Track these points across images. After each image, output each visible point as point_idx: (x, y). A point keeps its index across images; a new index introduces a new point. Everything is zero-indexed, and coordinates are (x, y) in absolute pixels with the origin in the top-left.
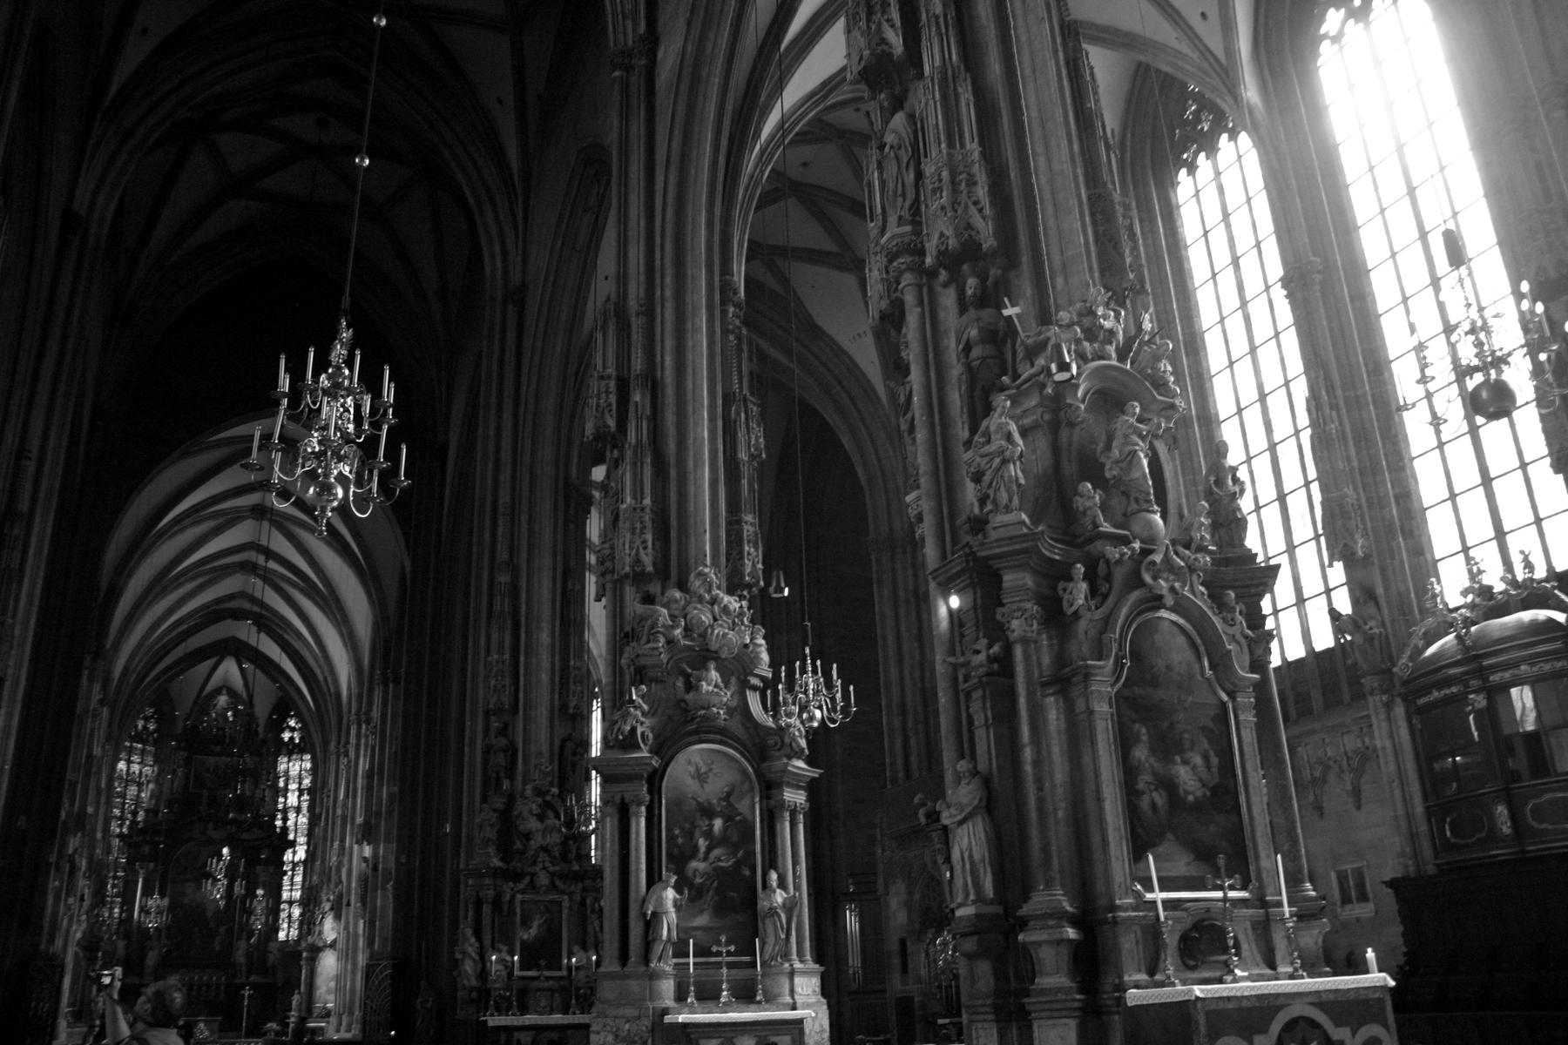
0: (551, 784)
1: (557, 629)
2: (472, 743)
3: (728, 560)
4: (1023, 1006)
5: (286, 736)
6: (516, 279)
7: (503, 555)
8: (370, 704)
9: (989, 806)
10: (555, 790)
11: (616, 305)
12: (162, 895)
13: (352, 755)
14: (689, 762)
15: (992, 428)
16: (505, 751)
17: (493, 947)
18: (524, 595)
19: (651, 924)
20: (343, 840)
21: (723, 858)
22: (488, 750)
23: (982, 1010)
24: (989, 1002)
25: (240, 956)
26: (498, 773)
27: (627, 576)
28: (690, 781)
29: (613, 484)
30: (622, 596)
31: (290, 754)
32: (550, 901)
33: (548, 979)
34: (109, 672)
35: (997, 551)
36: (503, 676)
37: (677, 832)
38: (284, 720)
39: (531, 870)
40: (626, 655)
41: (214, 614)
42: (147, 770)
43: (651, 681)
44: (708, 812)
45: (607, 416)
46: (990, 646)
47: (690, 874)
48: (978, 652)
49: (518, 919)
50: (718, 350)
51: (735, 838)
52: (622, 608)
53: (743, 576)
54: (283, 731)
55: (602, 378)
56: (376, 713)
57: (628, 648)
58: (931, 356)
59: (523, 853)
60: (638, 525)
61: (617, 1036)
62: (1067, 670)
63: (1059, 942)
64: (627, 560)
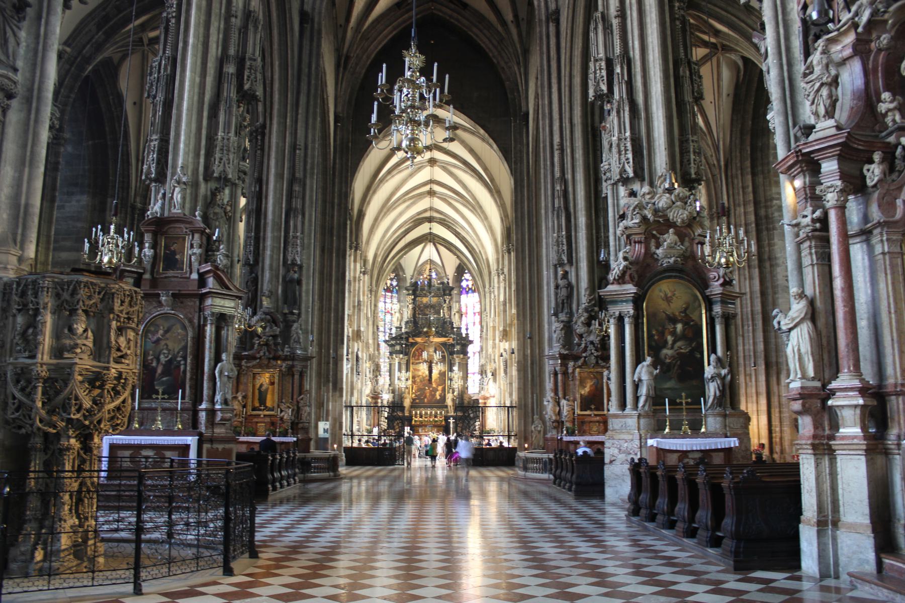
0: (594, 305)
1: (593, 214)
2: (548, 284)
3: (681, 165)
4: (830, 446)
5: (464, 284)
6: (552, 6)
7: (557, 174)
8: (503, 264)
9: (812, 315)
10: (596, 309)
11: (602, 13)
12: (407, 370)
13: (496, 293)
14: (660, 291)
15: (815, 63)
16: (567, 288)
17: (565, 398)
18: (571, 196)
19: (636, 386)
20: (494, 340)
21: (682, 346)
22: (557, 287)
23: (805, 447)
24: (809, 442)
25: (449, 402)
26: (563, 300)
27: (619, 181)
28: (661, 302)
29: (608, 125)
30: (617, 193)
31: (467, 293)
32: (597, 372)
33: (596, 415)
34: (366, 256)
35: (817, 147)
36: (563, 244)
37: (654, 333)
38: (463, 276)
39: (584, 355)
40: (620, 229)
41: (418, 221)
42: (396, 307)
43: (635, 242)
44: (673, 320)
45: (601, 84)
46: (813, 212)
47: (662, 356)
48: (806, 216)
49: (577, 383)
50: (669, 32)
51: (690, 335)
52: (618, 200)
53: (690, 174)
54: (462, 281)
55: (596, 60)
56: (506, 270)
57: (621, 224)
58: (780, 17)
59: (579, 345)
60: (622, 148)
61: (620, 450)
62: (869, 225)
63: (856, 406)
64: (618, 170)
